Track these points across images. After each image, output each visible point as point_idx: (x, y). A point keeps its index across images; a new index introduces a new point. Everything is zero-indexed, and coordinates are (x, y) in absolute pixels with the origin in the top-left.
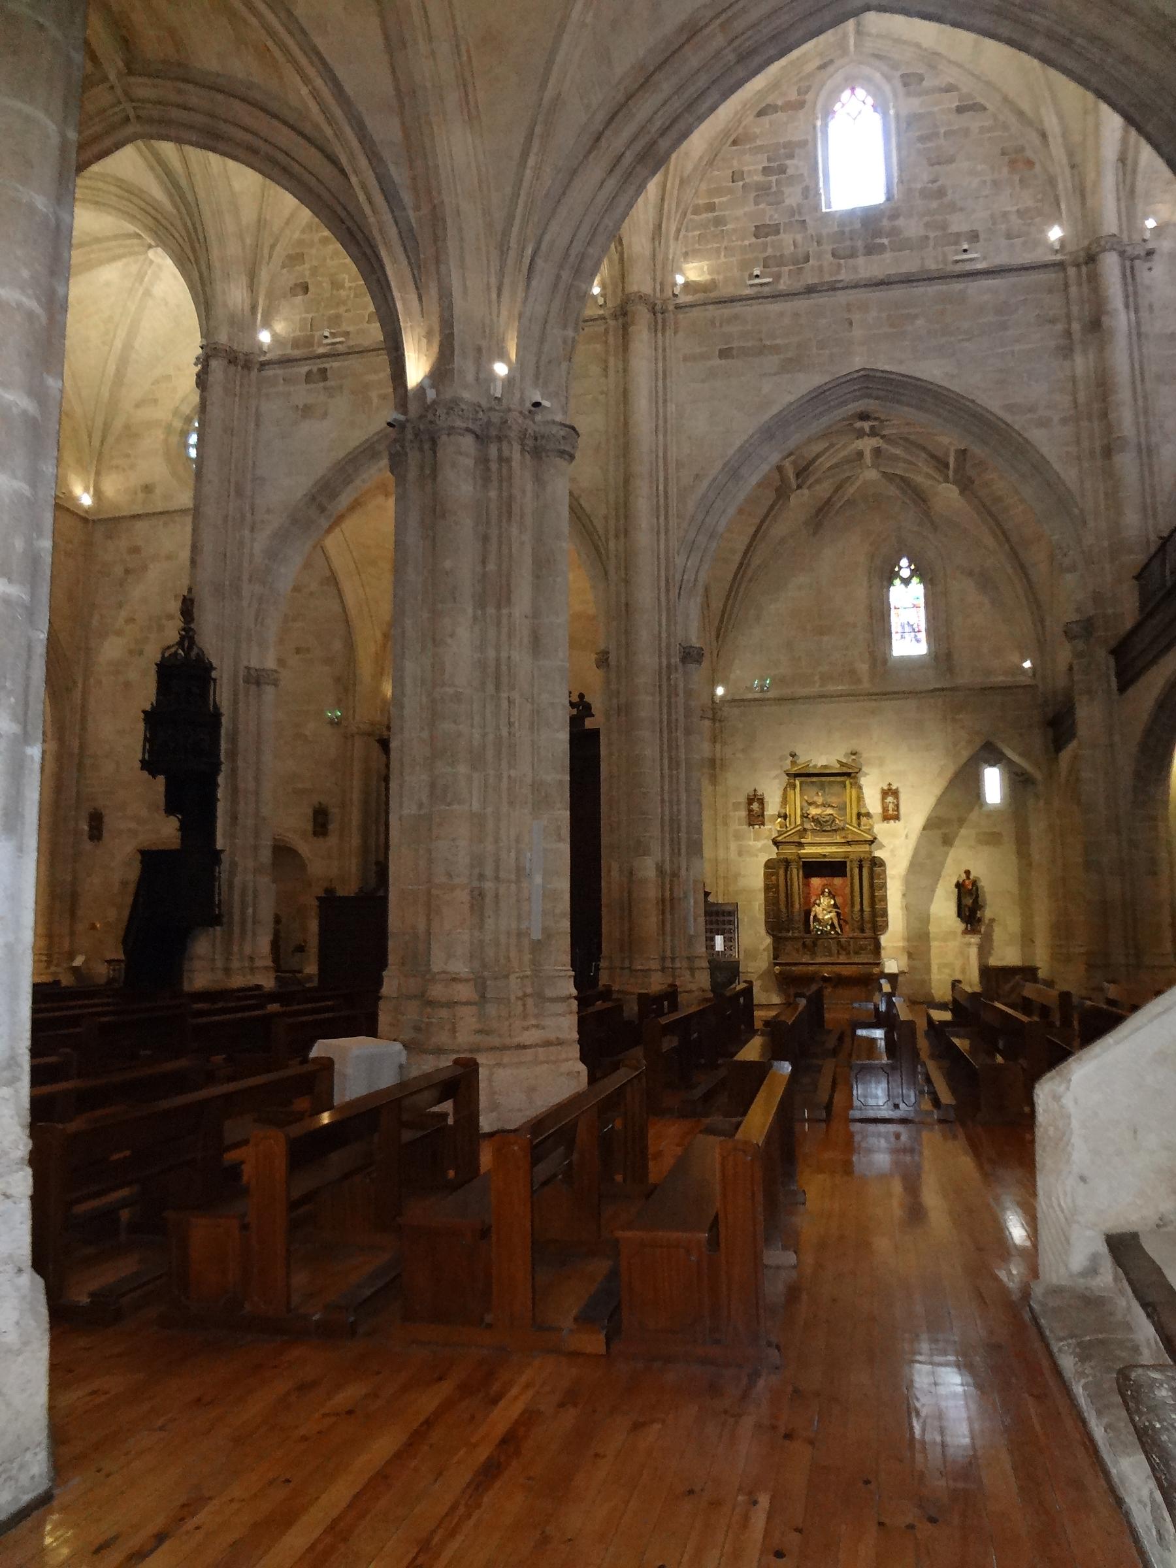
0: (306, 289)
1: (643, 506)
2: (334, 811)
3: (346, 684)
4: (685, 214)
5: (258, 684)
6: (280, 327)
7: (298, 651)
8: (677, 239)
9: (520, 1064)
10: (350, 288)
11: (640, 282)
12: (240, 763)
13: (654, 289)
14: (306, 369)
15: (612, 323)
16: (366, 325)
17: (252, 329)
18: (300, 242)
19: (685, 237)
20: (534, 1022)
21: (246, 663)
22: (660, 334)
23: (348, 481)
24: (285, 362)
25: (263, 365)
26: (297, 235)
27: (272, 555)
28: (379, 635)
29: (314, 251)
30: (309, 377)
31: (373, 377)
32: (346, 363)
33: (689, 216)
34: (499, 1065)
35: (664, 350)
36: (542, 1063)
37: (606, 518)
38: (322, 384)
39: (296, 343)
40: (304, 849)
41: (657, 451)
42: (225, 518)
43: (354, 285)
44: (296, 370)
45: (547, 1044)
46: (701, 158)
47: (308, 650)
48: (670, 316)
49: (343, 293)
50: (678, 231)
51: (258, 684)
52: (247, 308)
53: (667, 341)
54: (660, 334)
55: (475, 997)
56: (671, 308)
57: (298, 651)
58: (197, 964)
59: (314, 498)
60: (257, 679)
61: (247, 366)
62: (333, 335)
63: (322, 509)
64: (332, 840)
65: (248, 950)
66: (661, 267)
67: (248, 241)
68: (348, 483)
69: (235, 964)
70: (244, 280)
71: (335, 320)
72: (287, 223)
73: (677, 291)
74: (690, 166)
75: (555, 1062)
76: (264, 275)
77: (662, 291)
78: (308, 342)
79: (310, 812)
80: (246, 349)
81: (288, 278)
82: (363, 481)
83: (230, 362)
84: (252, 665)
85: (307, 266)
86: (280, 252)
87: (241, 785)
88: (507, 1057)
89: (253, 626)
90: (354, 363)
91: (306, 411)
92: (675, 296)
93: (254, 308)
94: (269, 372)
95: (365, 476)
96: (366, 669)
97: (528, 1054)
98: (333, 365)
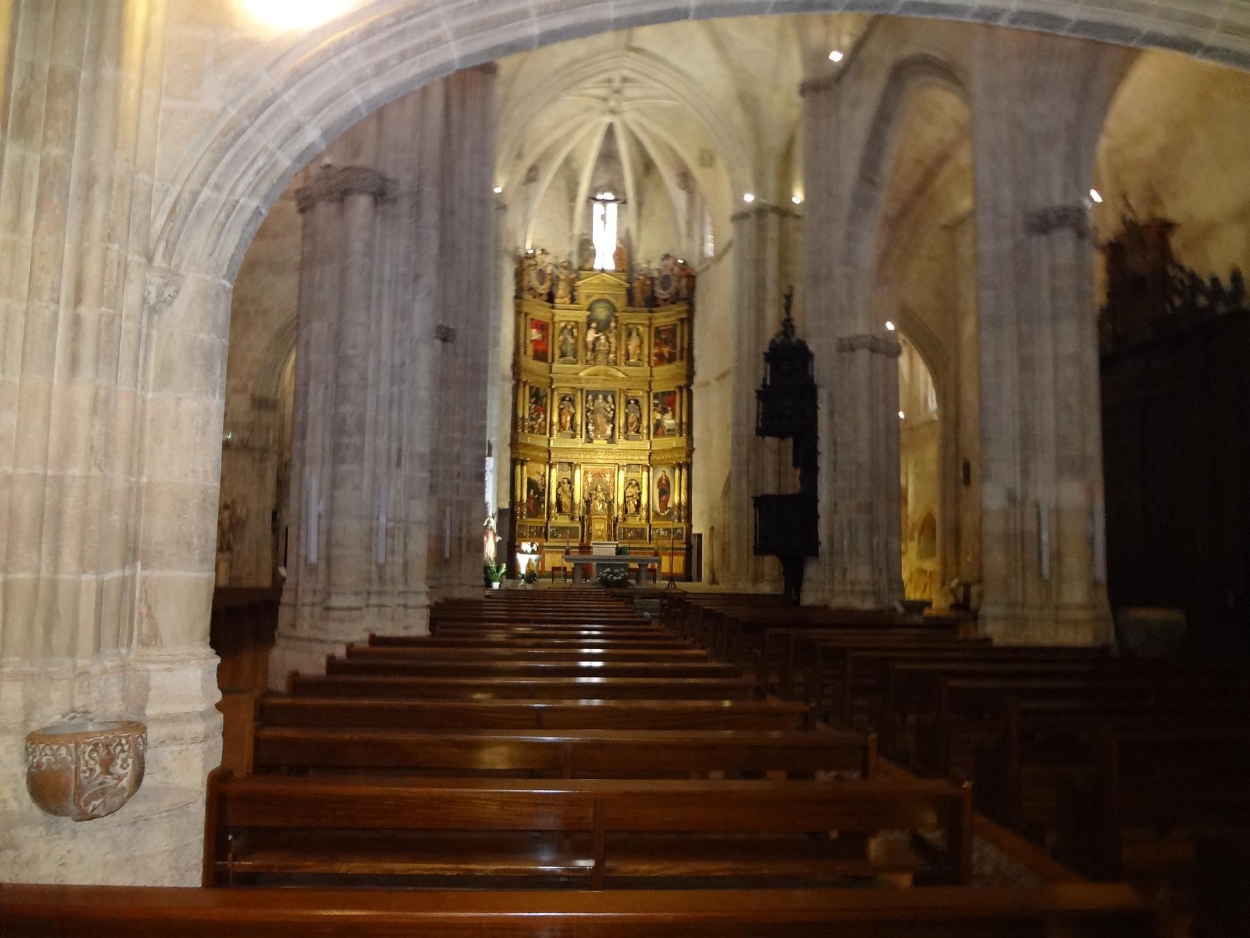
51: (852, 350)
58: (806, 586)
60: (847, 347)
65: (850, 576)
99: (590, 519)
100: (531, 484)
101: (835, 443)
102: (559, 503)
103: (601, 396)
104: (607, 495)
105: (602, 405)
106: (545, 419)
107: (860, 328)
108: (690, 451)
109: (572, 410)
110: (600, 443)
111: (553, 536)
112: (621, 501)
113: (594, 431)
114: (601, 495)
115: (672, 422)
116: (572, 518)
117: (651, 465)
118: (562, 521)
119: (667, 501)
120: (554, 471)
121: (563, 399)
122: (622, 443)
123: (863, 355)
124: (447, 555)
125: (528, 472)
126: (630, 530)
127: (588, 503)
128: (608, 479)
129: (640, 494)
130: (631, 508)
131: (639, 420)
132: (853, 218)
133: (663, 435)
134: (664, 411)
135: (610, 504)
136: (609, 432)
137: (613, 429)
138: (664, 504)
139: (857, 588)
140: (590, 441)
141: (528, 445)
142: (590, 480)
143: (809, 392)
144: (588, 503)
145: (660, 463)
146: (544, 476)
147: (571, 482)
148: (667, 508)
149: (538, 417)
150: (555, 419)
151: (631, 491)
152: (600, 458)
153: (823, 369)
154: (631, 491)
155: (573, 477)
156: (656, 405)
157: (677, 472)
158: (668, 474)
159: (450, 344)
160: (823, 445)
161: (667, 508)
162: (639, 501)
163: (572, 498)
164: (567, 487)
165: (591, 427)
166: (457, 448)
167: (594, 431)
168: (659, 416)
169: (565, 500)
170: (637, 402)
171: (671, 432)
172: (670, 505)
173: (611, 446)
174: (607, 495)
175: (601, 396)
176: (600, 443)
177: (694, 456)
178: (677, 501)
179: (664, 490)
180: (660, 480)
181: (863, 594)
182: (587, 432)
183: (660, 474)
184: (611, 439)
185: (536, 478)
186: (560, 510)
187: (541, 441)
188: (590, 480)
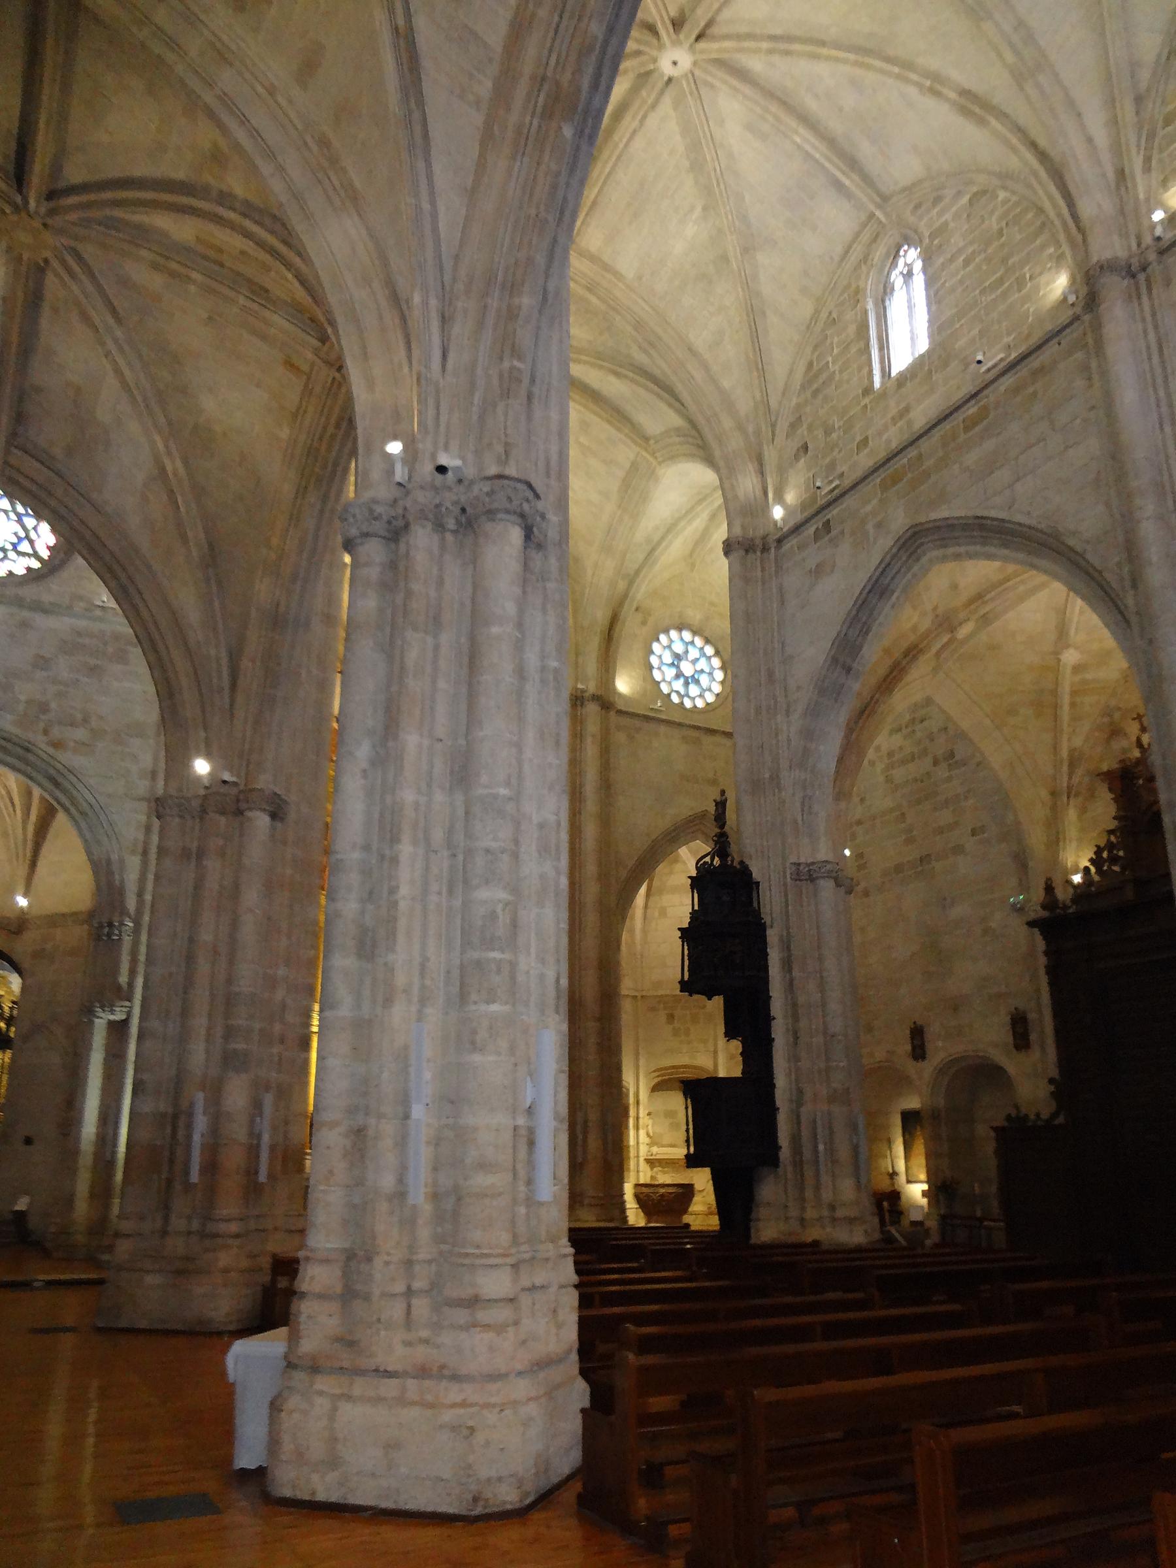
0: (805, 448)
1: (1149, 531)
2: (1032, 1016)
3: (1021, 860)
4: (1151, 136)
5: (812, 879)
6: (791, 497)
7: (974, 833)
8: (1147, 169)
9: (379, 1400)
10: (839, 428)
11: (1108, 246)
12: (796, 973)
13: (1129, 247)
14: (813, 529)
15: (1087, 318)
16: (856, 457)
17: (766, 509)
18: (799, 407)
19: (1160, 161)
20: (424, 1334)
21: (793, 859)
22: (1145, 298)
23: (865, 631)
24: (797, 529)
25: (780, 541)
26: (794, 401)
27: (808, 734)
28: (1044, 794)
29: (808, 409)
30: (817, 536)
31: (869, 508)
32: (844, 506)
33: (1161, 133)
34: (349, 1398)
35: (1154, 315)
36: (413, 1403)
37: (1119, 564)
38: (826, 539)
39: (803, 506)
40: (1012, 1064)
41: (1165, 445)
42: (758, 710)
43: (841, 423)
44: (806, 534)
45: (422, 1372)
46: (1159, 56)
47: (983, 829)
48: (1155, 269)
49: (834, 435)
50: (1148, 160)
51: (812, 879)
52: (759, 493)
53: (1156, 302)
54: (1145, 298)
55: (339, 1289)
56: (1152, 256)
57: (974, 833)
58: (762, 1212)
59: (835, 660)
60: (806, 875)
61: (765, 549)
62: (831, 482)
63: (848, 670)
64: (1036, 1054)
65: (827, 1195)
66: (1129, 211)
67: (750, 429)
68: (867, 633)
69: (810, 1213)
70: (751, 467)
71: (832, 466)
72: (784, 394)
73: (1159, 231)
74: (1145, 75)
75: (431, 1406)
76: (771, 456)
77: (1139, 245)
78: (814, 499)
79: (1008, 1019)
80: (761, 532)
81: (794, 444)
82: (880, 624)
83: (747, 551)
84: (802, 860)
85: (805, 426)
86: (783, 426)
87: (801, 999)
88: (359, 1387)
89: (799, 818)
90: (850, 501)
91: (818, 571)
92: (1159, 239)
93: (765, 493)
94: (786, 546)
95: (881, 619)
96: (1036, 838)
97: (389, 1388)
98: (835, 512)
101: (795, 1005)
107: (823, 853)
123: (827, 887)
124: (262, 1177)
132: (813, 711)
139: (840, 1213)
143: (755, 931)
153: (771, 901)
159: (279, 825)
160: (777, 1007)
166: (280, 994)
181: (851, 1221)
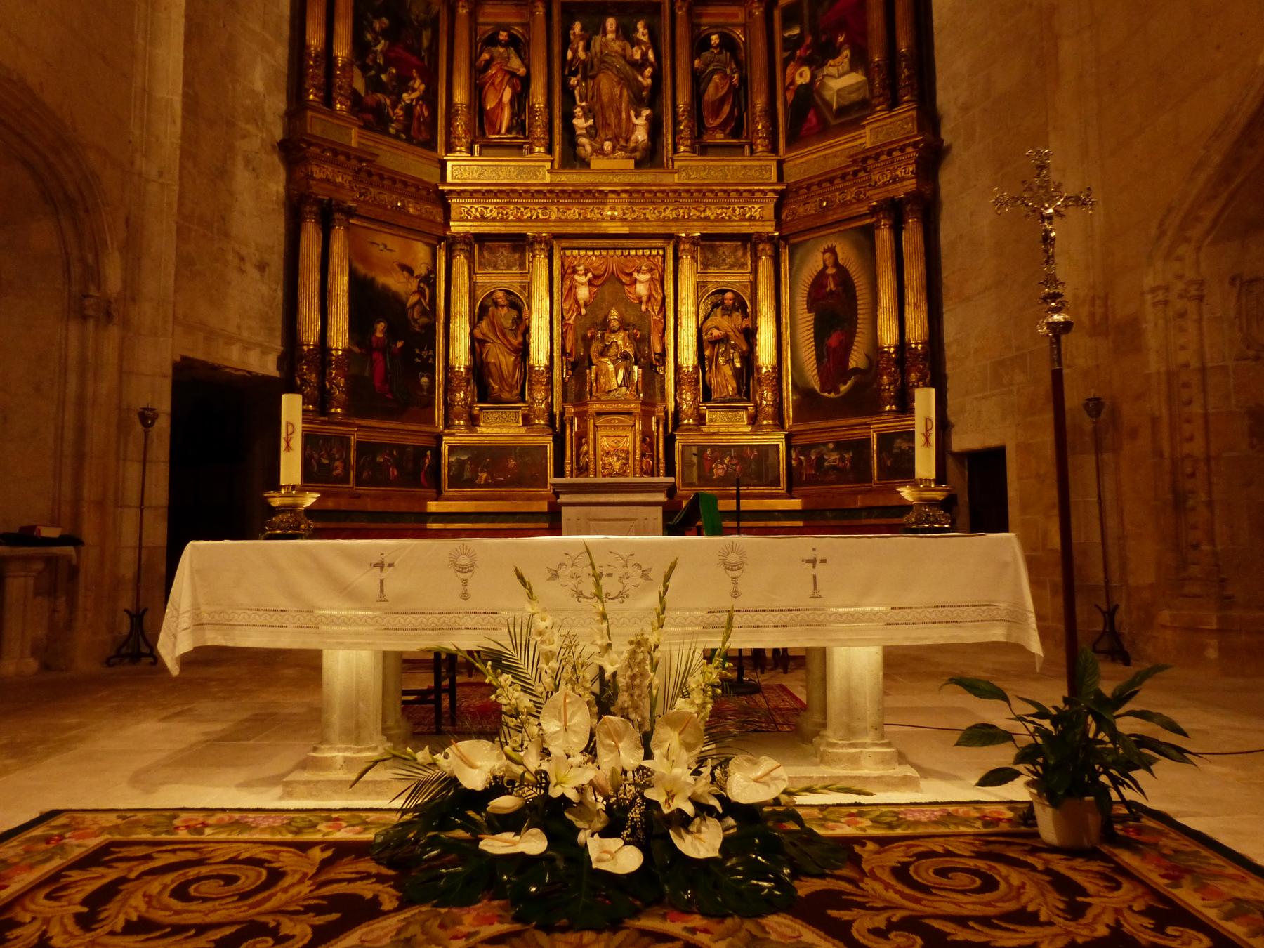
99: (583, 416)
100: (368, 302)
102: (479, 368)
103: (611, 23)
104: (641, 341)
105: (616, 46)
106: (430, 98)
108: (932, 157)
109: (515, 63)
110: (608, 167)
111: (456, 481)
112: (689, 358)
113: (592, 133)
114: (620, 341)
115: (855, 78)
116: (527, 421)
117: (785, 241)
118: (498, 429)
119: (847, 348)
120: (460, 262)
121: (492, 41)
122: (687, 168)
125: (358, 254)
126: (723, 450)
127: (578, 365)
128: (641, 289)
129: (750, 334)
130: (724, 380)
131: (740, 94)
133: (824, 131)
134: (820, 56)
135: (652, 365)
136: (641, 135)
137: (655, 128)
138: (832, 358)
140: (572, 158)
141: (338, 153)
142: (583, 293)
144: (578, 365)
145: (817, 227)
146: (429, 280)
147: (518, 306)
148: (845, 374)
149: (403, 83)
150: (460, 97)
151: (723, 324)
152: (612, 218)
154: (723, 324)
155: (527, 286)
156: (792, 45)
157: (884, 237)
158: (846, 254)
161: (845, 374)
162: (749, 357)
163: (523, 351)
164: (505, 316)
165: (580, 123)
167: (592, 133)
168: (803, 76)
169: (501, 358)
170: (728, 43)
171: (852, 114)
172: (856, 359)
173: (647, 177)
174: (641, 341)
175: (611, 23)
176: (608, 167)
177: (948, 179)
178: (887, 337)
179: (834, 310)
180: (820, 278)
182: (569, 129)
183: (815, 262)
184: (650, 157)
185: (396, 282)
186: (484, 394)
187: (414, 165)
188: (583, 293)
